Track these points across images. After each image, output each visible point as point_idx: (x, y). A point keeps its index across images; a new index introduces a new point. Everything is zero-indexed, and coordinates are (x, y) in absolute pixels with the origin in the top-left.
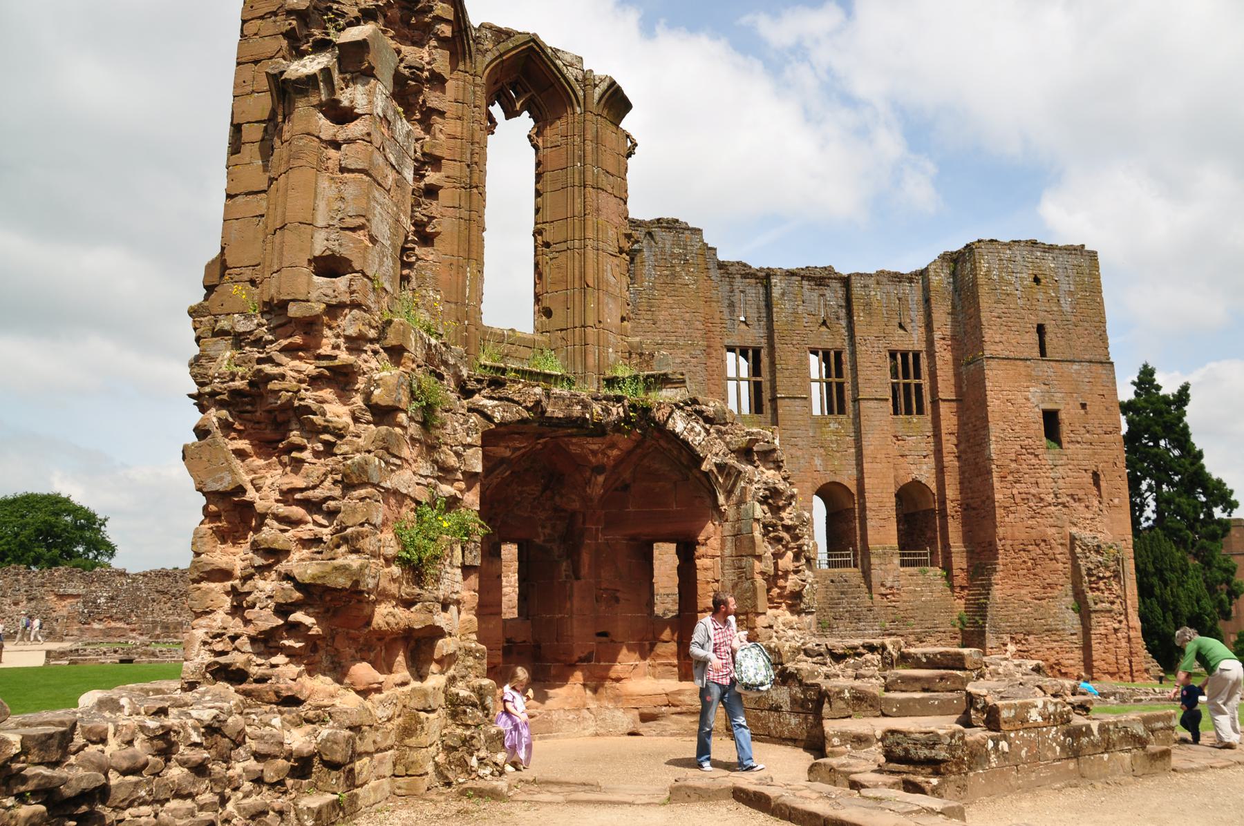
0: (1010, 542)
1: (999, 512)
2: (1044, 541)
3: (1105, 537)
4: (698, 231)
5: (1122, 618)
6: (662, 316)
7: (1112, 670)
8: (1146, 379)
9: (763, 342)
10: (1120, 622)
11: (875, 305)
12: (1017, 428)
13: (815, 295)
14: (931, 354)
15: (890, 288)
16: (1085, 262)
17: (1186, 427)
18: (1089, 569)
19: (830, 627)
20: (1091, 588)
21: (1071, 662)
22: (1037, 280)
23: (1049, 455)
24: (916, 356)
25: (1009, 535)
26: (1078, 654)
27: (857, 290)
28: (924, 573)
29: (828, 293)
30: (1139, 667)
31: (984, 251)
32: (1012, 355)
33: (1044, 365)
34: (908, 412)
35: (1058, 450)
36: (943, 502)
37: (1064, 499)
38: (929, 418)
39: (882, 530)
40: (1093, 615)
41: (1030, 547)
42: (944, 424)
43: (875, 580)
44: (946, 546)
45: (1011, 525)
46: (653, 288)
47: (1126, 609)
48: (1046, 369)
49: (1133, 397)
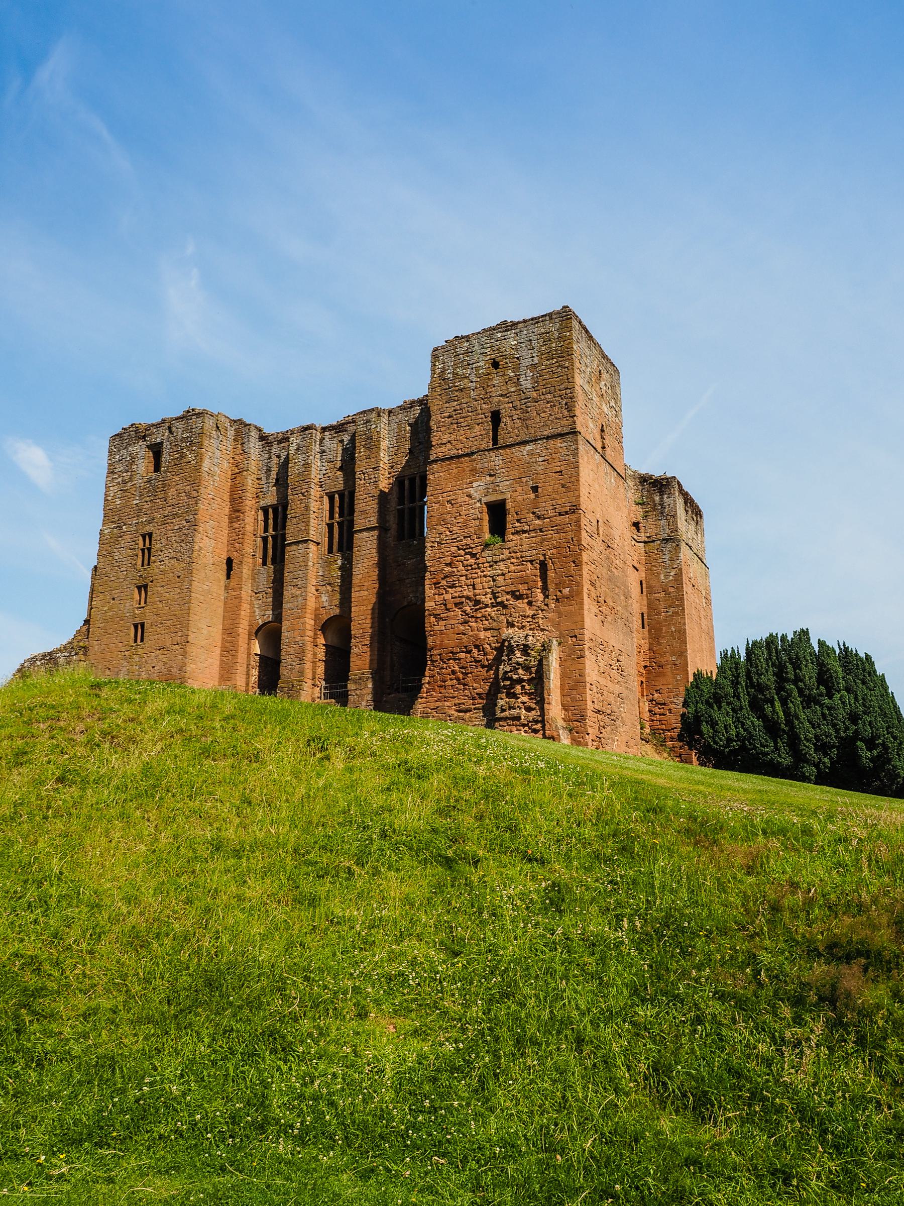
22: (495, 365)
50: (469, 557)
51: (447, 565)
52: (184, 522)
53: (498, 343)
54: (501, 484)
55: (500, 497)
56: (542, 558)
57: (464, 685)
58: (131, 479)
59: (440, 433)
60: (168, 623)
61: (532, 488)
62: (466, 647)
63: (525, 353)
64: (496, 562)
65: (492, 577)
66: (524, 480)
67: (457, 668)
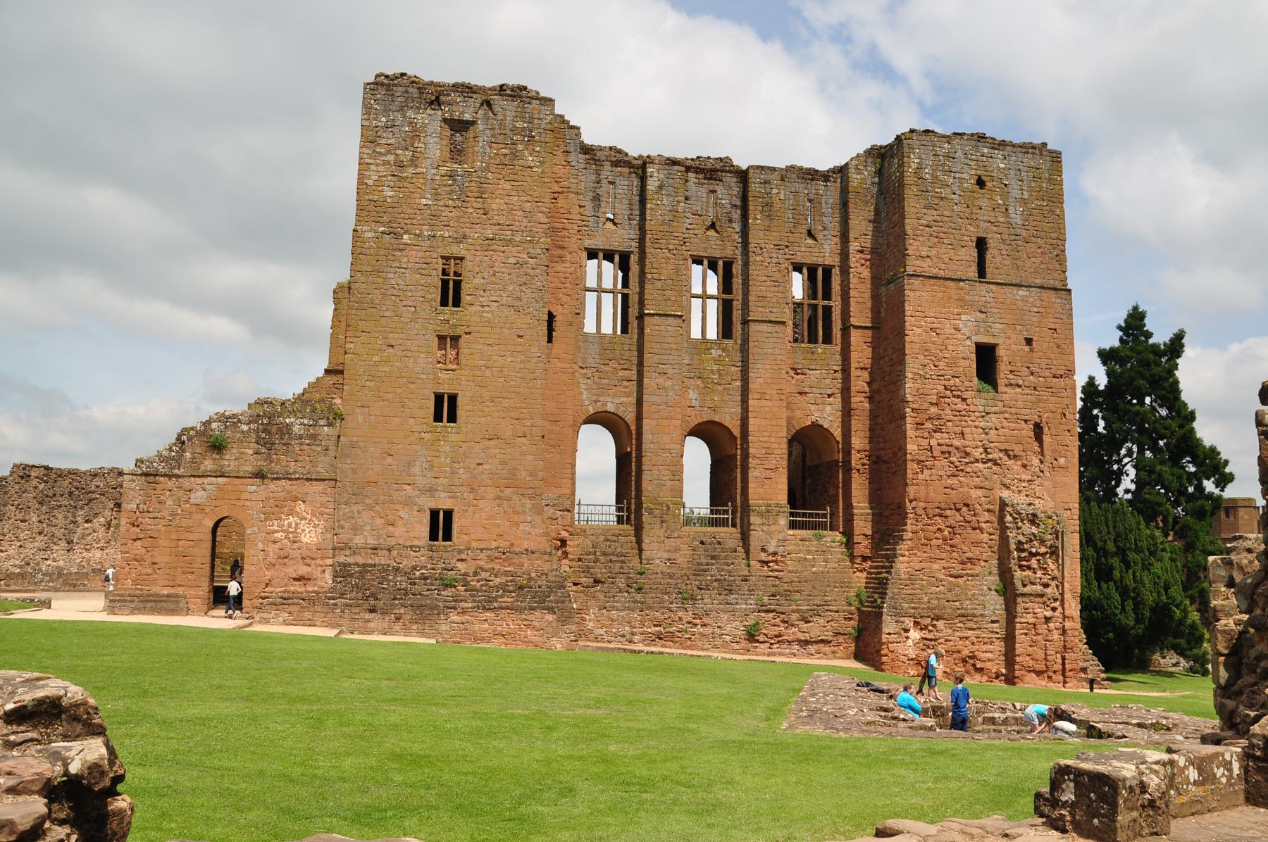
0: (922, 505)
1: (912, 467)
2: (967, 505)
3: (1044, 505)
4: (549, 102)
5: (1057, 604)
6: (496, 204)
7: (1039, 667)
8: (1134, 324)
9: (634, 245)
10: (1054, 609)
11: (777, 206)
12: (942, 364)
13: (703, 191)
14: (845, 270)
15: (800, 187)
16: (1044, 164)
17: (1177, 382)
18: (1020, 542)
19: (693, 598)
20: (1021, 567)
21: (989, 655)
22: (981, 183)
23: (980, 400)
24: (827, 271)
25: (922, 495)
26: (999, 647)
27: (755, 187)
28: (821, 537)
29: (720, 189)
30: (1074, 666)
31: (915, 143)
32: (941, 274)
33: (982, 288)
34: (813, 339)
35: (992, 394)
36: (847, 452)
37: (995, 455)
38: (838, 348)
39: (768, 483)
40: (1019, 600)
41: (948, 512)
42: (854, 357)
43: (754, 544)
44: (849, 506)
45: (925, 484)
46: (487, 169)
47: (1062, 594)
48: (983, 293)
49: (1117, 344)
58: (414, 162)
60: (505, 403)
63: (1012, 181)
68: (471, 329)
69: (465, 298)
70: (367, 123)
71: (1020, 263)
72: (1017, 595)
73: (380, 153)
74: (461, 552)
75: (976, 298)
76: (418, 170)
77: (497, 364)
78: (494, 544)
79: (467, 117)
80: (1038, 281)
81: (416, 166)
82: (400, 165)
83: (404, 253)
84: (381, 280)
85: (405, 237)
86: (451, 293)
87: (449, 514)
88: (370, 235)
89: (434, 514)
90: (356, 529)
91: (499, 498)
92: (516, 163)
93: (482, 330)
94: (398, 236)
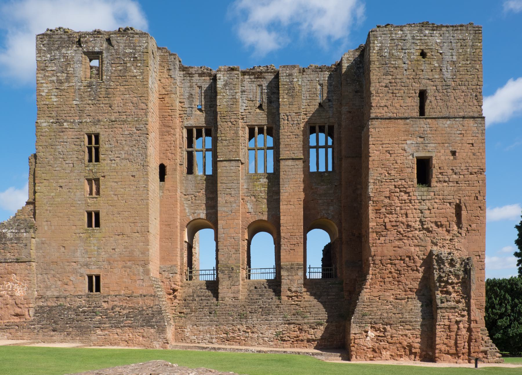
22: (423, 54)
33: (422, 122)
46: (110, 80)
50: (403, 194)
51: (386, 197)
52: (134, 129)
53: (426, 38)
54: (429, 145)
55: (428, 155)
56: (458, 202)
57: (399, 282)
58: (68, 79)
59: (378, 98)
60: (126, 214)
61: (452, 152)
62: (401, 256)
64: (424, 200)
65: (421, 210)
66: (446, 145)
67: (393, 270)
68: (105, 174)
69: (101, 157)
70: (39, 59)
71: (449, 104)
72: (438, 308)
73: (48, 76)
74: (104, 297)
75: (418, 129)
76: (71, 84)
77: (121, 193)
78: (123, 292)
79: (97, 49)
80: (461, 114)
81: (69, 82)
82: (61, 82)
83: (65, 133)
84: (52, 150)
85: (65, 124)
86: (94, 154)
87: (98, 278)
88: (45, 124)
89: (90, 277)
90: (47, 288)
91: (125, 267)
92: (127, 74)
93: (111, 174)
94: (61, 124)
